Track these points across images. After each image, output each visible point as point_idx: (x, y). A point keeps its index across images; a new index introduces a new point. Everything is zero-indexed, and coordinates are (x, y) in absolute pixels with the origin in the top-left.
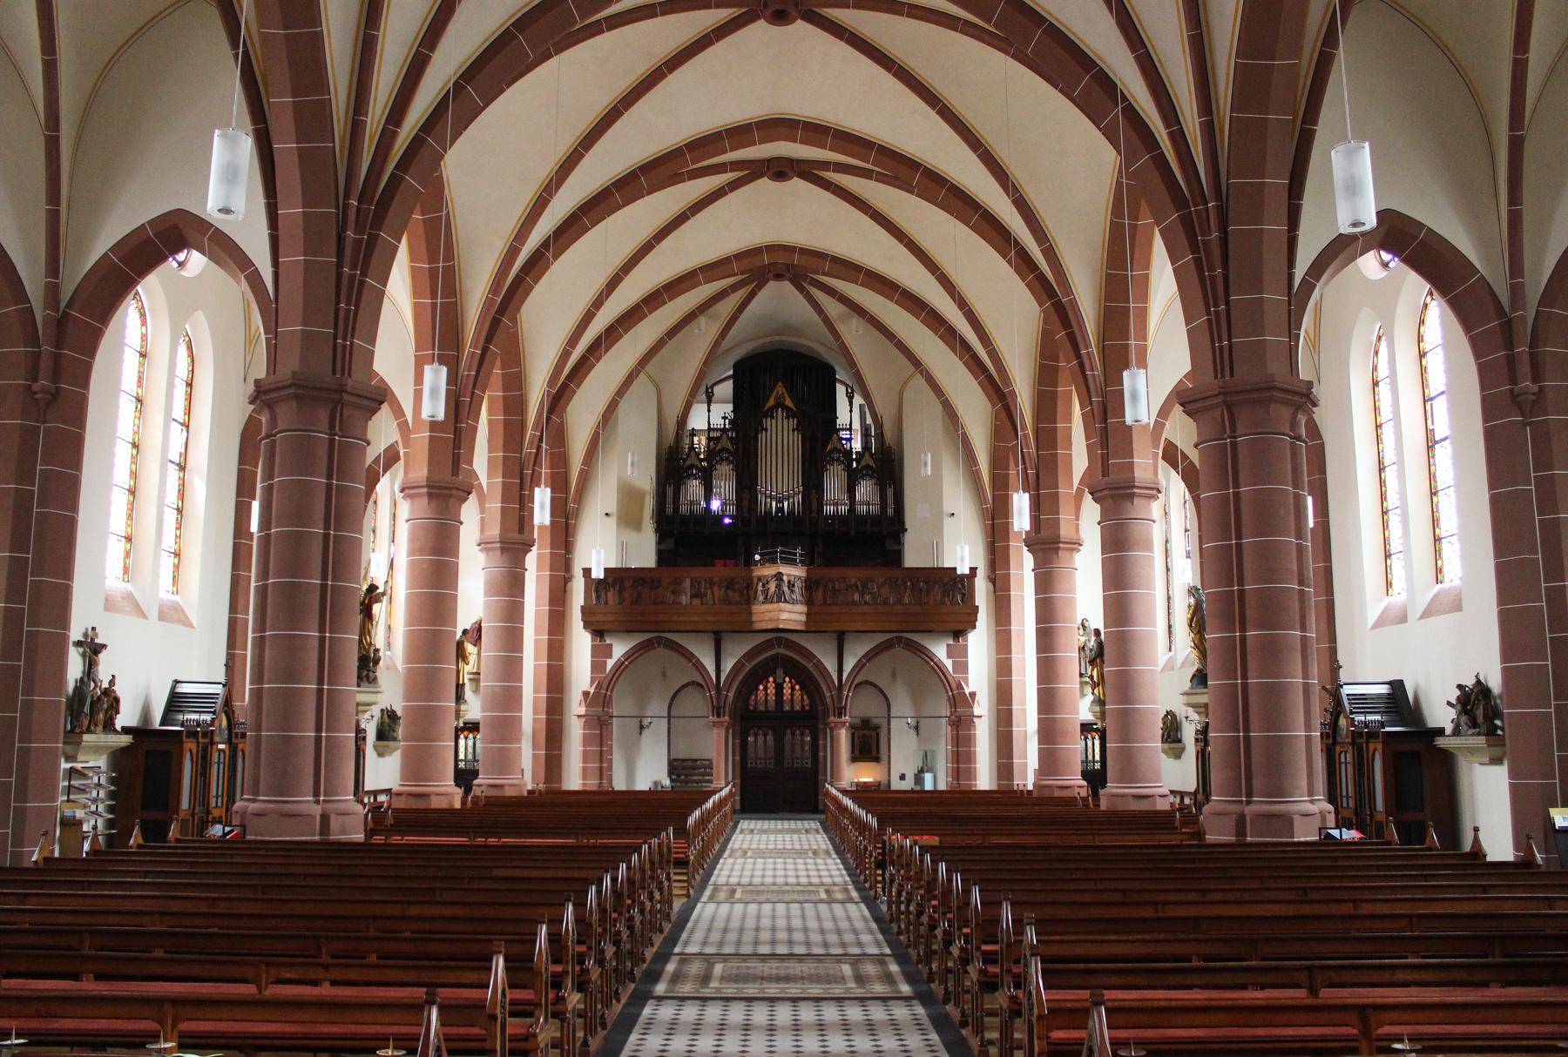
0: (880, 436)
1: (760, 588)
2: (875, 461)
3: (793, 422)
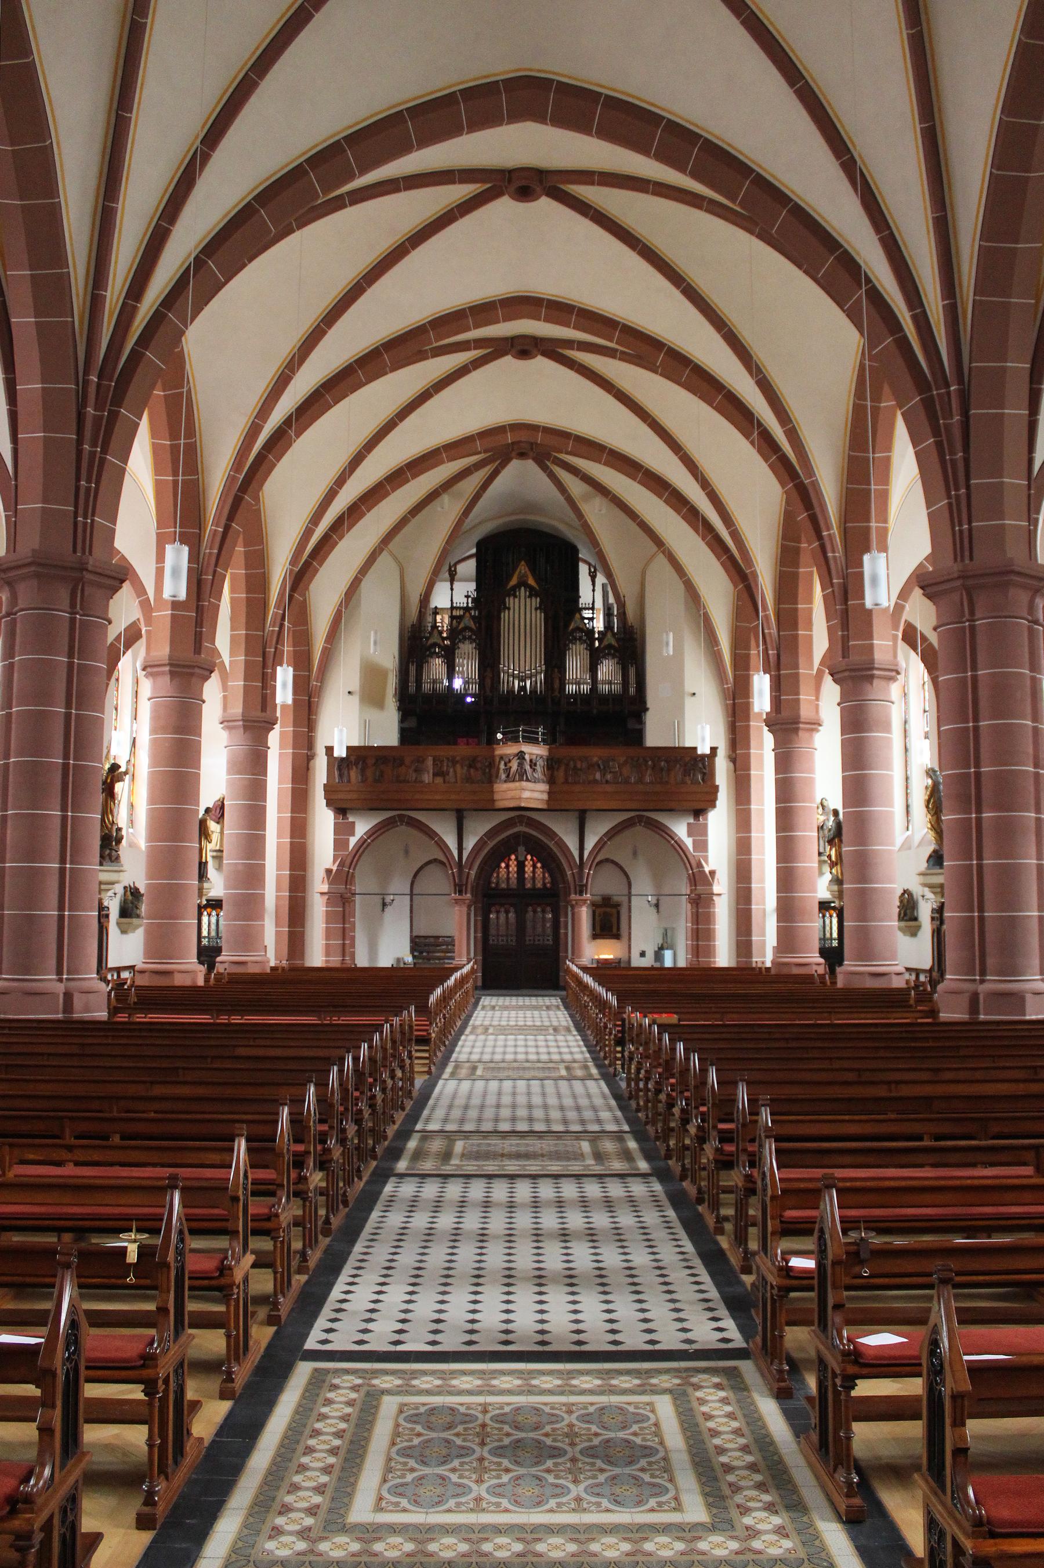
0: (623, 615)
2: (618, 640)
3: (536, 602)
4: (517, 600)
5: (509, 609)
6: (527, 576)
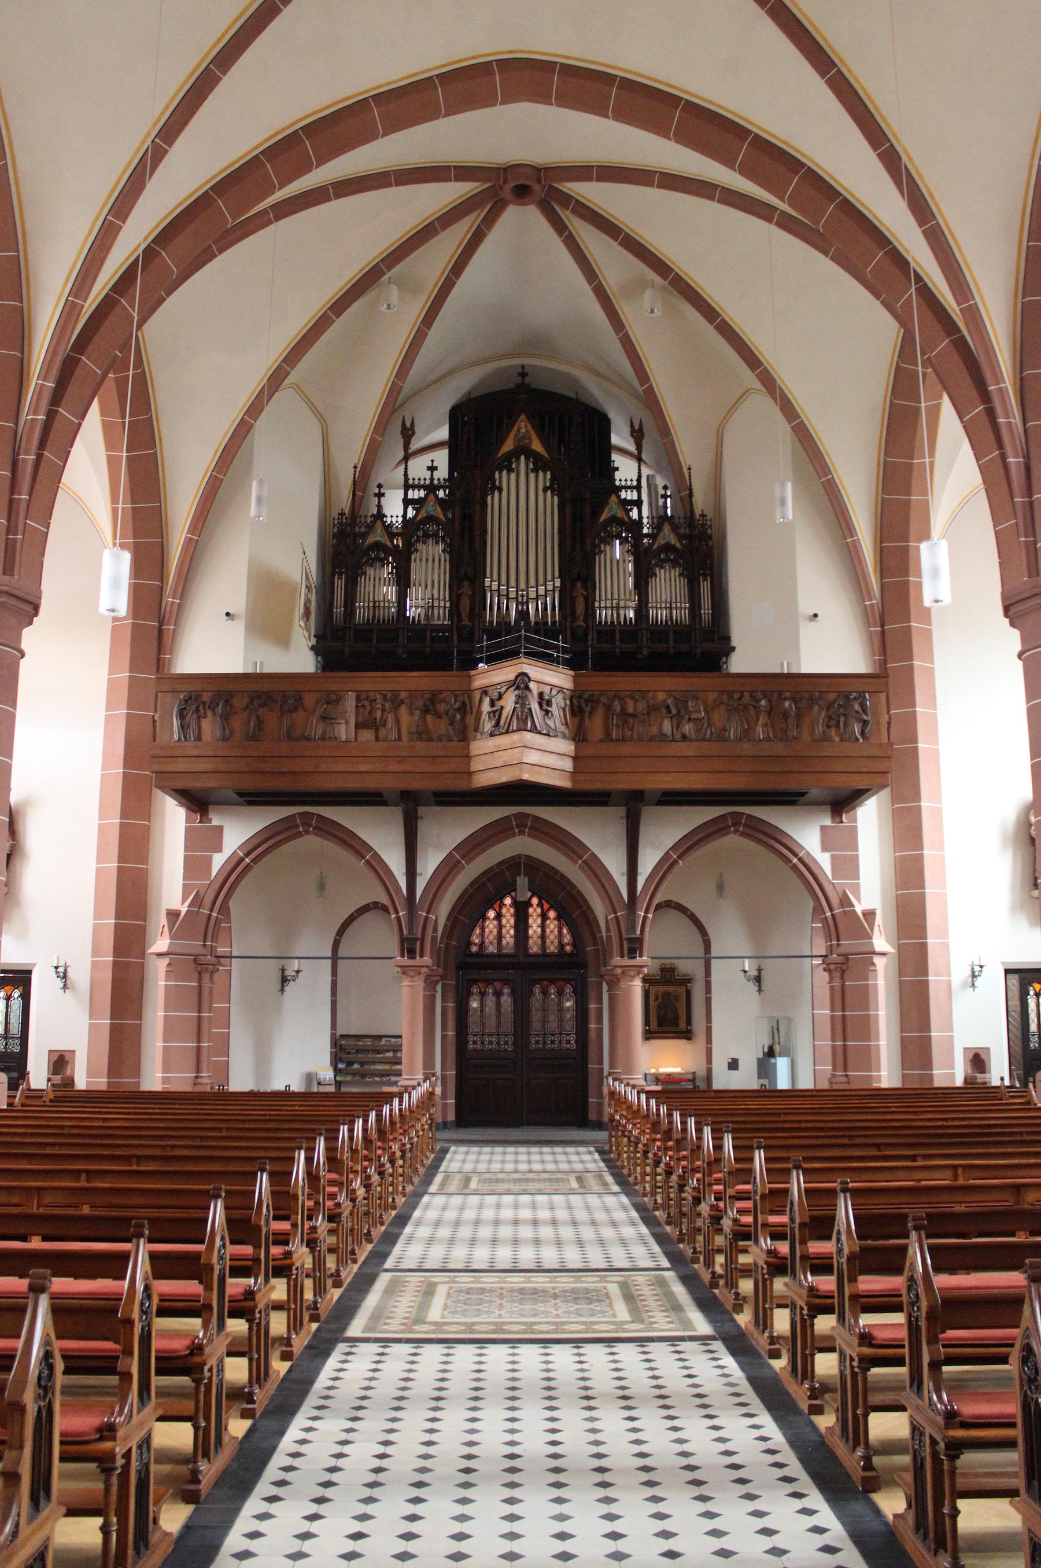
1: (486, 707)
3: (544, 478)
4: (513, 476)
5: (500, 490)
6: (529, 438)
